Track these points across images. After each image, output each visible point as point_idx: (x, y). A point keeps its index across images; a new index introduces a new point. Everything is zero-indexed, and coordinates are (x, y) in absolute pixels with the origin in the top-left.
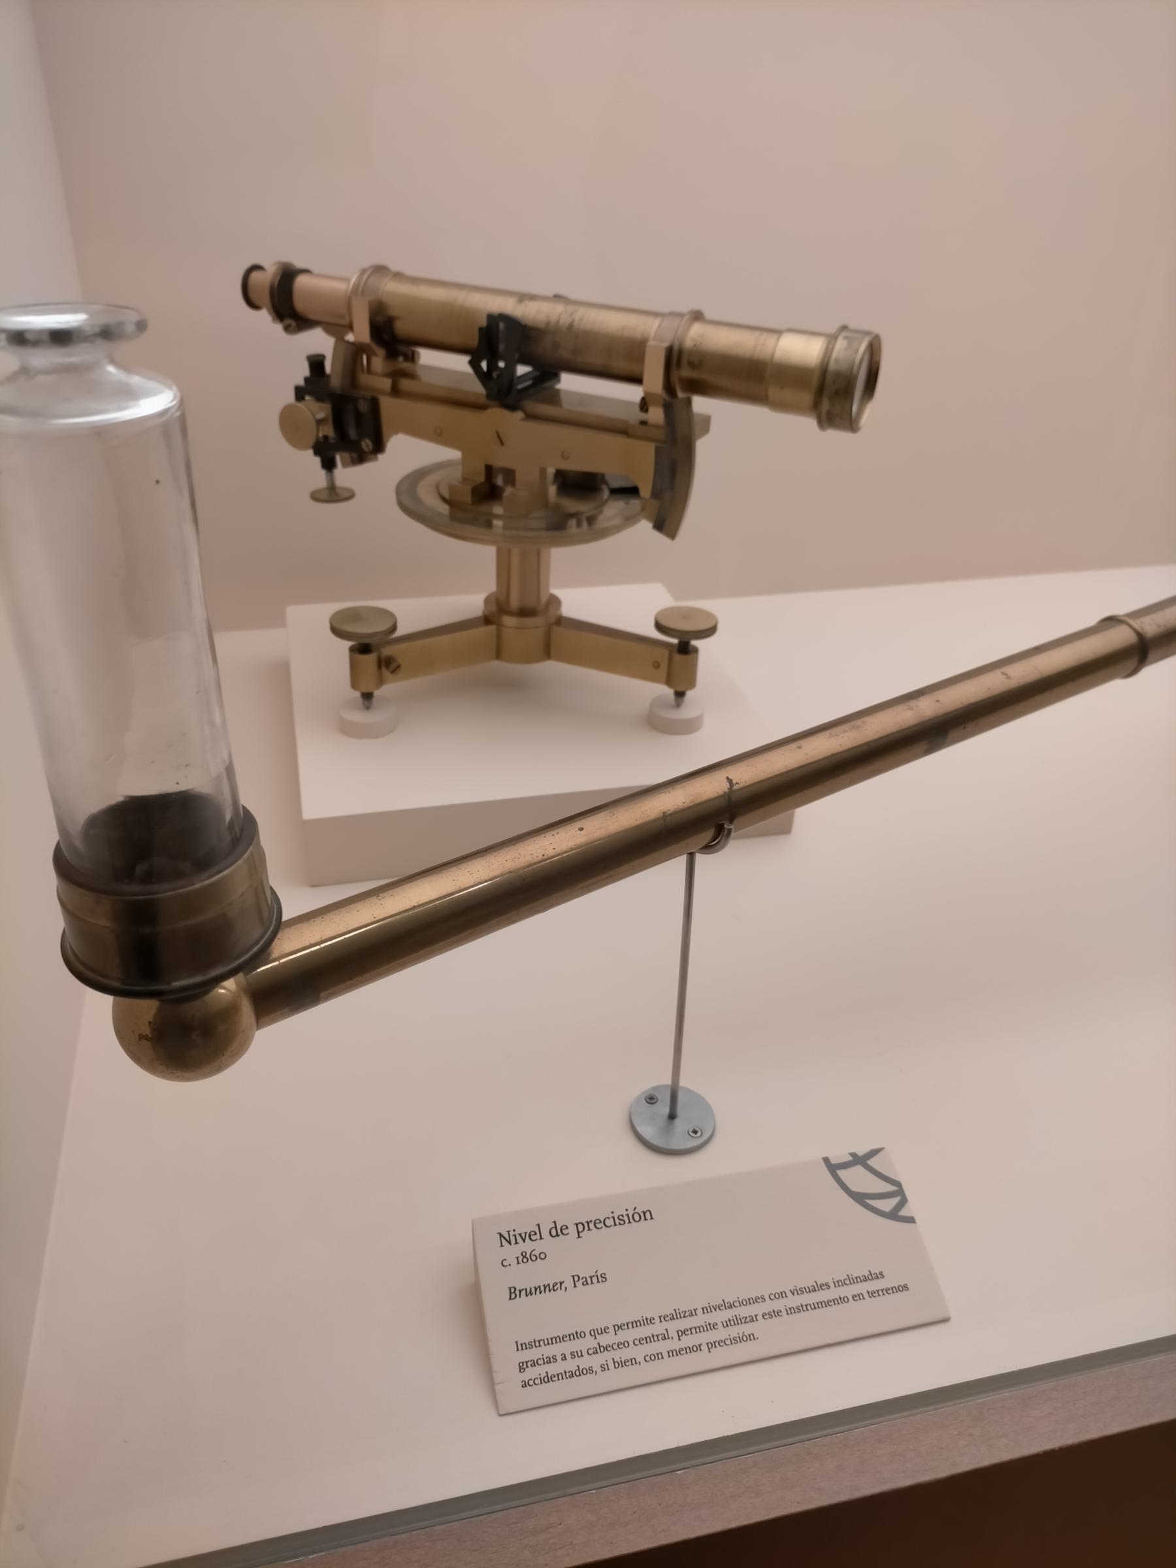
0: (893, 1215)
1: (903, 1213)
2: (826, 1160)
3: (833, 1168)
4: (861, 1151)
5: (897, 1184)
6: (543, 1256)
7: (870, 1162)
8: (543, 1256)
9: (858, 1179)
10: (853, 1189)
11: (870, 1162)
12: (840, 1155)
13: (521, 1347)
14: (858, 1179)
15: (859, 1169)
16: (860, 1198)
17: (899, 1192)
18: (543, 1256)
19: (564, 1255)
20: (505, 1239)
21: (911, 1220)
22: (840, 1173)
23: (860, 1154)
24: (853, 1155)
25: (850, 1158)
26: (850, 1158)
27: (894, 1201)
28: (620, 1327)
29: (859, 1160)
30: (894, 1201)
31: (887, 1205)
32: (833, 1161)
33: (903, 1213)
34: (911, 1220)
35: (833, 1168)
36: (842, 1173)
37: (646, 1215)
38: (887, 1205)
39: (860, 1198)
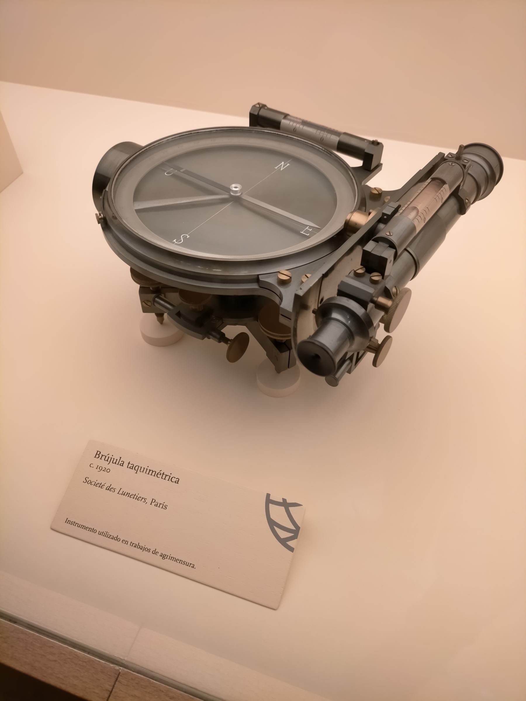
0: (283, 542)
1: (290, 543)
2: (268, 495)
3: (269, 501)
5: (298, 528)
6: (108, 471)
7: (291, 509)
8: (108, 471)
9: (278, 514)
10: (272, 517)
11: (291, 509)
12: (276, 497)
14: (278, 514)
15: (282, 509)
16: (272, 524)
17: (296, 532)
18: (108, 471)
20: (98, 455)
21: (291, 549)
22: (271, 506)
23: (288, 501)
24: (284, 500)
25: (282, 501)
26: (282, 501)
27: (291, 535)
29: (286, 504)
30: (291, 535)
31: (284, 535)
32: (271, 498)
33: (290, 543)
34: (291, 549)
35: (269, 501)
36: (271, 506)
38: (284, 535)
39: (272, 524)
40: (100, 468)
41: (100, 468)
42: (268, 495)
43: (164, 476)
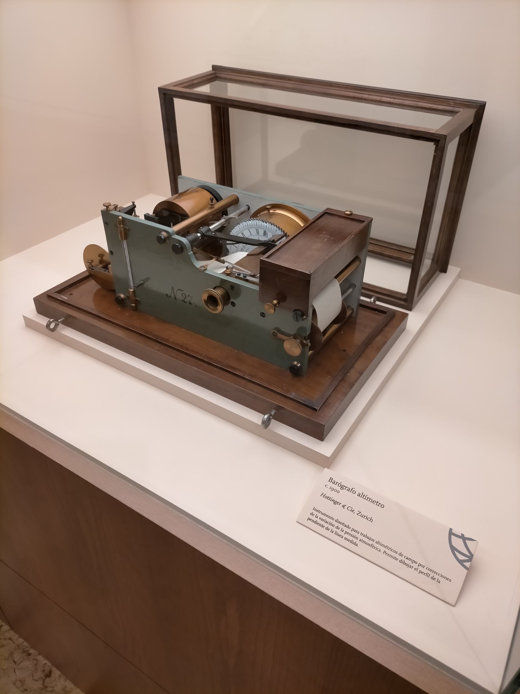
0: (461, 562)
2: (451, 530)
3: (451, 533)
4: (466, 536)
6: (338, 492)
7: (466, 541)
9: (458, 543)
11: (466, 541)
12: (457, 531)
13: (314, 509)
14: (458, 543)
16: (453, 549)
17: (471, 557)
19: (343, 497)
24: (463, 535)
28: (421, 565)
29: (462, 537)
35: (451, 533)
37: (383, 506)
39: (453, 549)
40: (333, 490)
41: (333, 490)
42: (451, 530)
43: (378, 504)
